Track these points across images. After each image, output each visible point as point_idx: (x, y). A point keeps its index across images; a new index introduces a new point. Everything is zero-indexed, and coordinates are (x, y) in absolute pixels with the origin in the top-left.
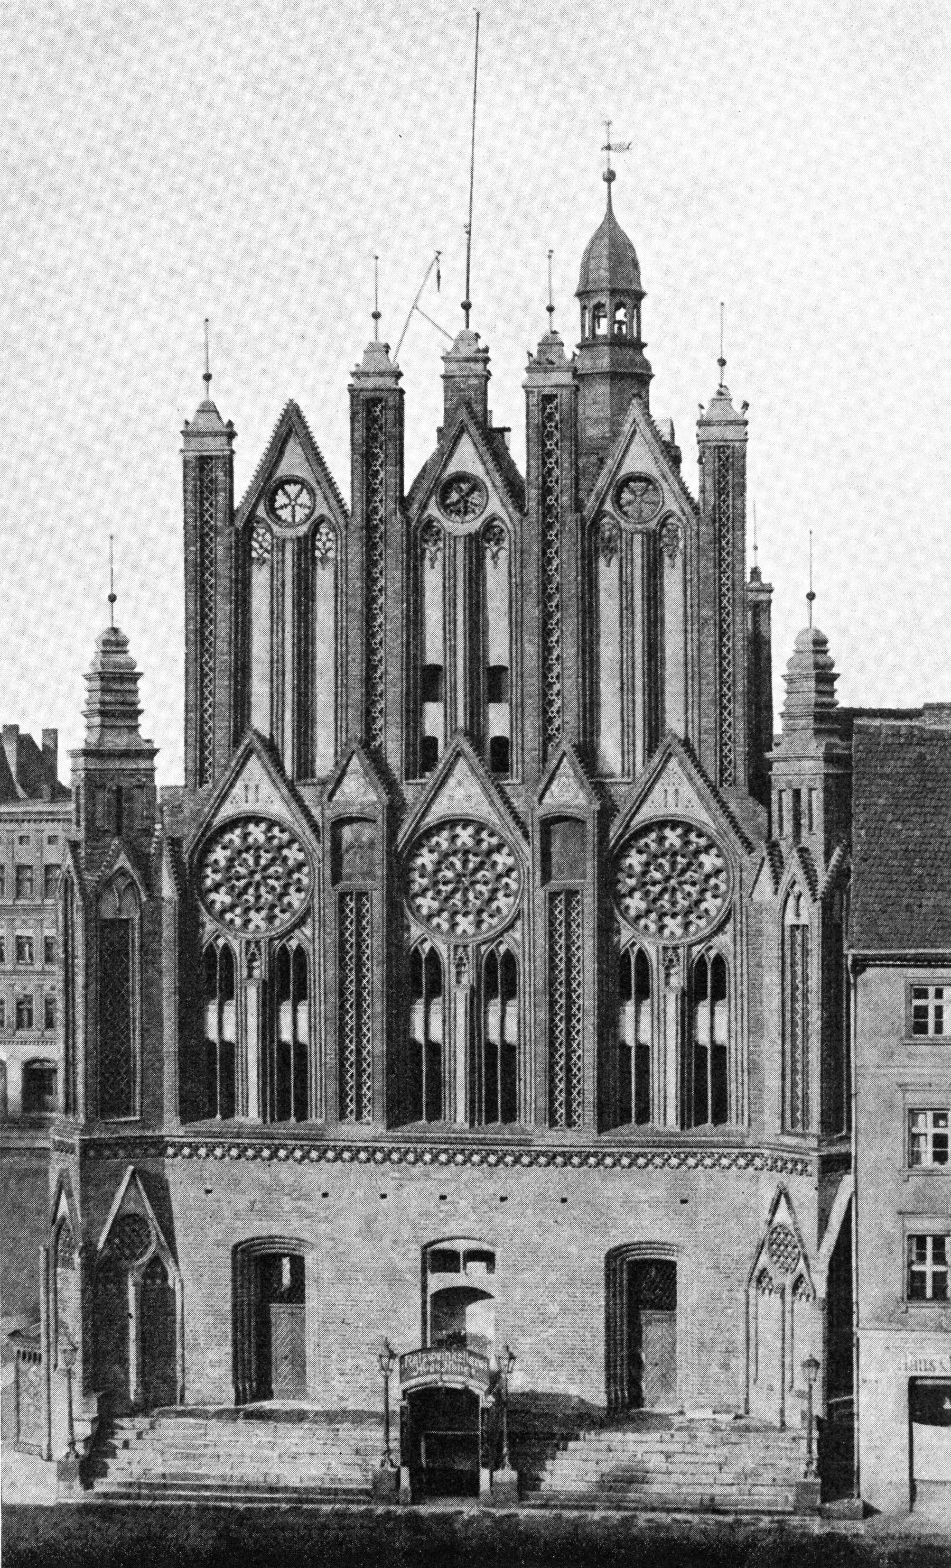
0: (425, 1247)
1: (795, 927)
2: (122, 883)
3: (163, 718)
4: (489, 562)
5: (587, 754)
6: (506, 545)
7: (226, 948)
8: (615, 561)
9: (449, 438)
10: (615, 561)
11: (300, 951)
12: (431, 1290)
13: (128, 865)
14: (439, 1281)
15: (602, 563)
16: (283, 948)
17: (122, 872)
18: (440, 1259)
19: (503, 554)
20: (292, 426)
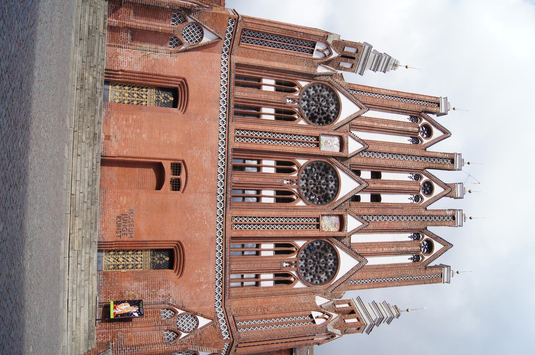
0: (183, 161)
1: (311, 316)
2: (327, 52)
3: (371, 79)
4: (409, 196)
5: (359, 231)
6: (415, 202)
7: (295, 91)
8: (410, 239)
9: (445, 186)
10: (410, 239)
11: (294, 119)
12: (163, 162)
13: (332, 57)
14: (167, 166)
15: (410, 235)
16: (294, 113)
17: (331, 54)
18: (177, 168)
19: (412, 201)
20: (446, 134)
